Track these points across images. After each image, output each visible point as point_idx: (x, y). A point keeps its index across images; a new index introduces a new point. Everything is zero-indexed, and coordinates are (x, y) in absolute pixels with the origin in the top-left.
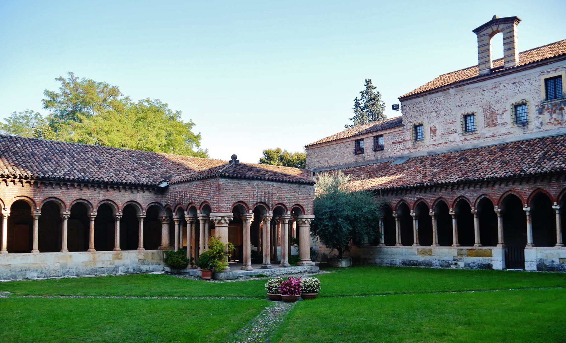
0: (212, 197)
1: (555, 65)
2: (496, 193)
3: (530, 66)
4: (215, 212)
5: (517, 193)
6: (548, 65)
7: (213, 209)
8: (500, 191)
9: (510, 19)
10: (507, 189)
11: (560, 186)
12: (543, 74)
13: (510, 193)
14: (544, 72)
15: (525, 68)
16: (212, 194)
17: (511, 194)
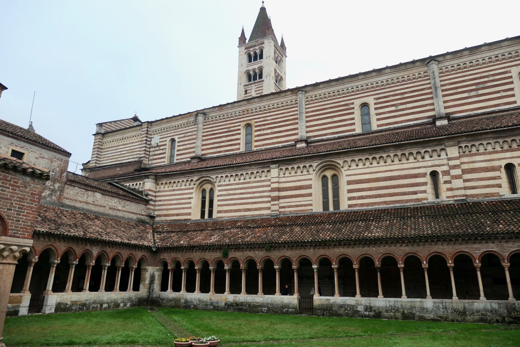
0: (15, 207)
1: (23, 144)
2: (39, 245)
3: (7, 133)
4: (19, 237)
5: (55, 248)
6: (18, 141)
7: (13, 230)
8: (44, 244)
9: (2, 86)
10: (49, 243)
11: (82, 248)
12: (12, 145)
13: (49, 247)
14: (13, 144)
15: (2, 133)
16: (14, 200)
17: (50, 248)
